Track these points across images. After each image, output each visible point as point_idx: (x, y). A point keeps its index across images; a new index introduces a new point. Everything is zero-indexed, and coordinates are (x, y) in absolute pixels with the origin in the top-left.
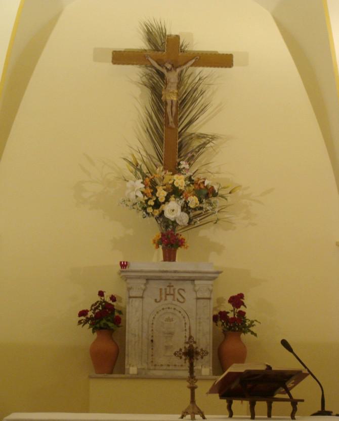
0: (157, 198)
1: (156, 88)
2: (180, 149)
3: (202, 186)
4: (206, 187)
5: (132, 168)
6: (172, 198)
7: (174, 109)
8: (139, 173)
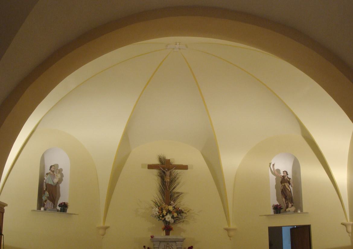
0: (163, 214)
1: (162, 176)
2: (171, 197)
3: (178, 210)
4: (180, 210)
5: (154, 204)
6: (168, 214)
7: (169, 184)
8: (157, 205)
